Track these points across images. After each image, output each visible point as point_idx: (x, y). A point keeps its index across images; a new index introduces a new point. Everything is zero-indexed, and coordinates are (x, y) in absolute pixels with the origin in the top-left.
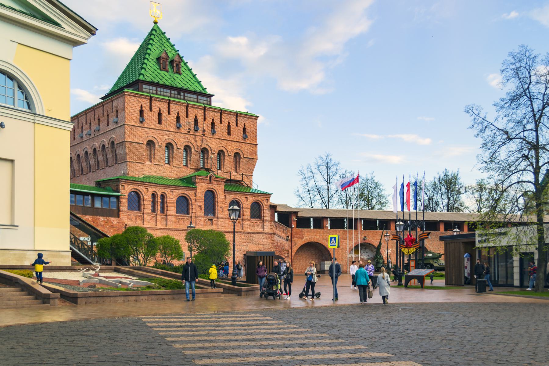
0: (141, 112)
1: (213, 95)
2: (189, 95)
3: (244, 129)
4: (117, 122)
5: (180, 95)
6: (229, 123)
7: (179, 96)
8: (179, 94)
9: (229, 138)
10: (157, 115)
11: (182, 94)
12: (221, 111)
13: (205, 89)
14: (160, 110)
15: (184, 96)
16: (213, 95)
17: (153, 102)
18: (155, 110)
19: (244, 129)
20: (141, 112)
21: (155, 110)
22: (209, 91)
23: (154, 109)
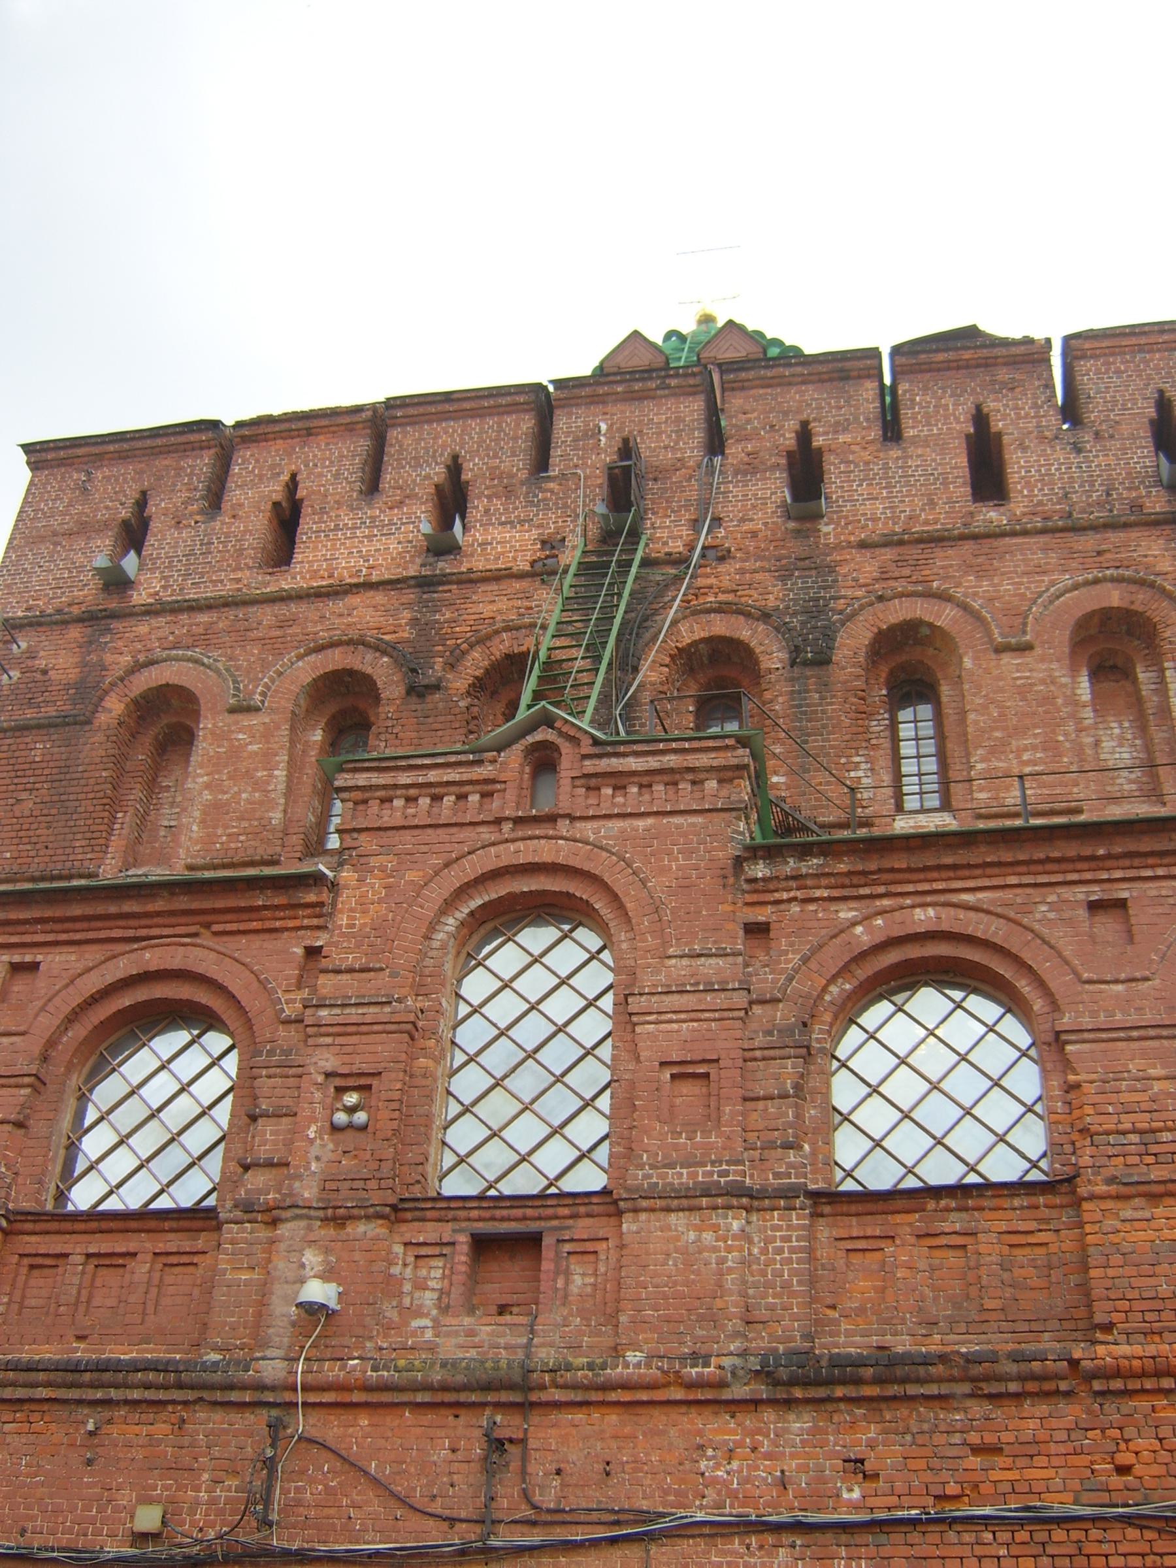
9: (992, 516)
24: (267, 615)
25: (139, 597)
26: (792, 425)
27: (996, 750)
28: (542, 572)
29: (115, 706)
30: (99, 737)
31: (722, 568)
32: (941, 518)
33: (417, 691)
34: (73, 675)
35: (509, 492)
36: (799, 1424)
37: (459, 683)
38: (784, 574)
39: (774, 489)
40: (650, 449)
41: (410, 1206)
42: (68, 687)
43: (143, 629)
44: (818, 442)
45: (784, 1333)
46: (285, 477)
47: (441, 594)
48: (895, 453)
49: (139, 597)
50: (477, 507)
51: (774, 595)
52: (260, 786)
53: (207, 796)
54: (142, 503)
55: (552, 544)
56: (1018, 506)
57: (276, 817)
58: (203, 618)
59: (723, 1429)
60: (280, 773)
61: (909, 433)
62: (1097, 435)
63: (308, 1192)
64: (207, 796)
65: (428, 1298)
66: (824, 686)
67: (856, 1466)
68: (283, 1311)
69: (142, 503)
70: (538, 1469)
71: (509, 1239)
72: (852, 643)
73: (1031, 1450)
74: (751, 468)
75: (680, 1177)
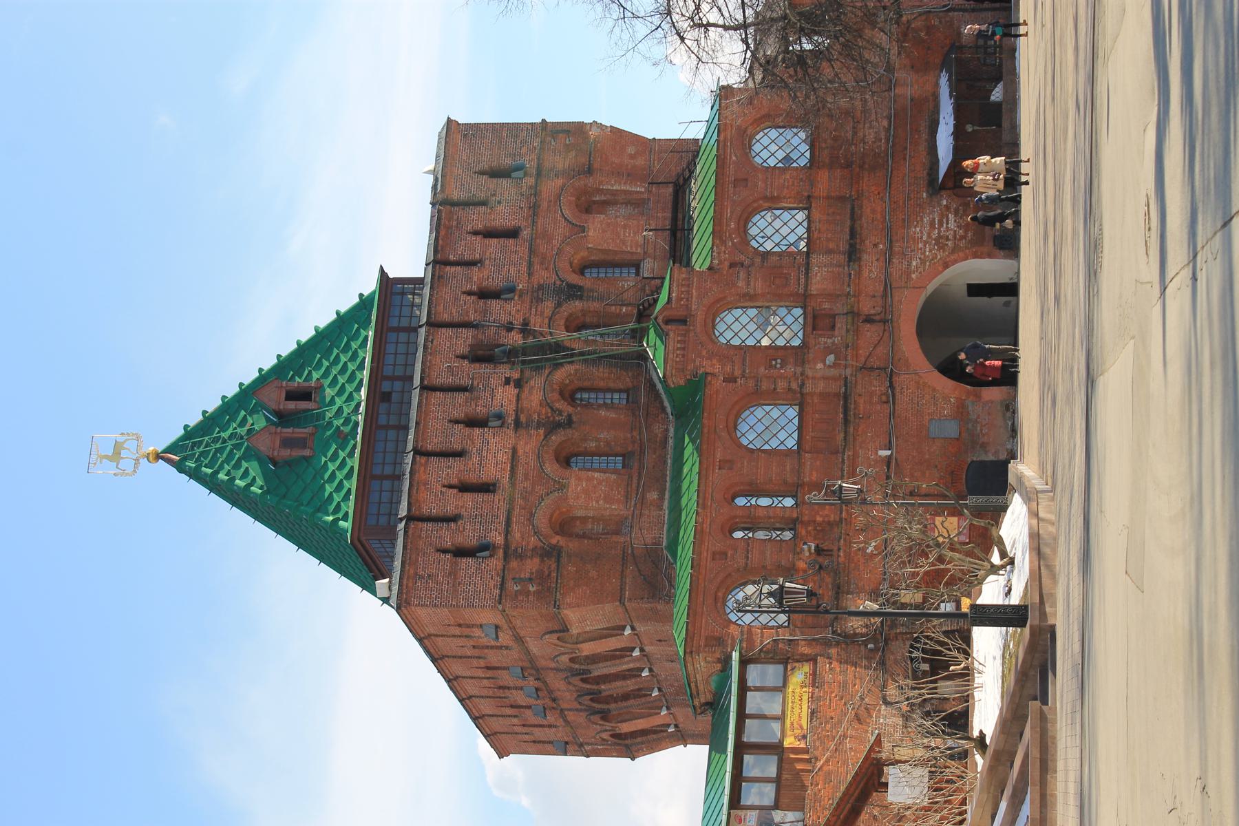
0: (461, 552)
1: (382, 272)
2: (390, 359)
3: (497, 173)
4: (497, 627)
5: (390, 394)
6: (476, 233)
7: (395, 397)
8: (386, 397)
9: (525, 233)
10: (468, 496)
11: (386, 386)
12: (439, 260)
13: (364, 303)
14: (451, 487)
15: (393, 379)
16: (382, 272)
17: (425, 511)
18: (454, 502)
19: (497, 173)
20: (461, 552)
21: (454, 502)
22: (370, 285)
23: (451, 509)
24: (521, 485)
25: (500, 540)
26: (464, 297)
27: (624, 244)
28: (519, 384)
29: (556, 539)
30: (570, 545)
31: (532, 321)
32: (523, 250)
33: (569, 423)
34: (537, 560)
35: (477, 399)
36: (865, 257)
37: (570, 409)
38: (540, 300)
39: (494, 305)
40: (464, 349)
41: (805, 345)
42: (542, 561)
43: (518, 535)
44: (475, 288)
45: (842, 258)
46: (444, 490)
47: (523, 418)
48: (487, 262)
49: (500, 540)
50: (481, 410)
51: (549, 305)
52: (600, 482)
53: (601, 502)
54: (445, 551)
55: (507, 381)
56: (523, 224)
57: (614, 477)
58: (516, 512)
59: (865, 273)
60: (596, 475)
61: (477, 256)
62: (494, 195)
63: (799, 370)
64: (601, 502)
65: (829, 341)
66: (592, 290)
67: (875, 245)
68: (833, 372)
69: (445, 551)
70: (872, 312)
71: (816, 322)
72: (574, 279)
73: (874, 211)
74: (485, 312)
75: (802, 281)
